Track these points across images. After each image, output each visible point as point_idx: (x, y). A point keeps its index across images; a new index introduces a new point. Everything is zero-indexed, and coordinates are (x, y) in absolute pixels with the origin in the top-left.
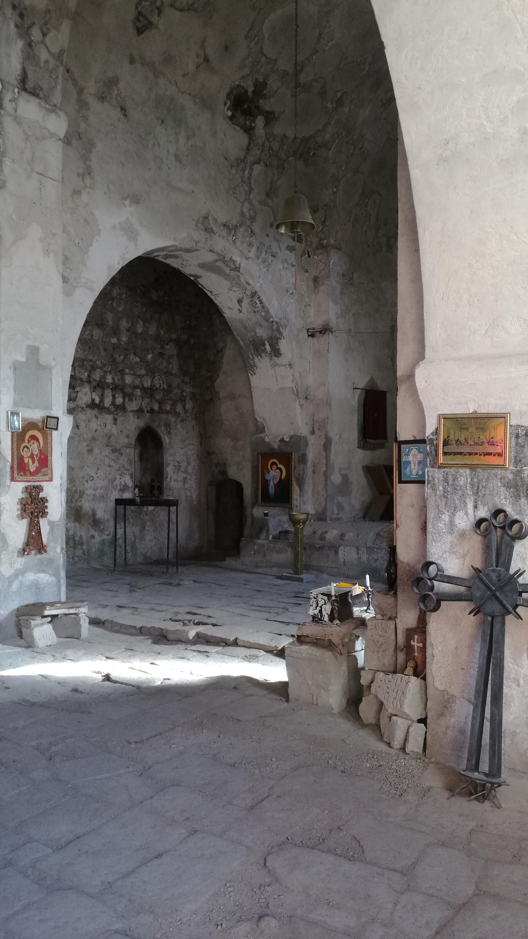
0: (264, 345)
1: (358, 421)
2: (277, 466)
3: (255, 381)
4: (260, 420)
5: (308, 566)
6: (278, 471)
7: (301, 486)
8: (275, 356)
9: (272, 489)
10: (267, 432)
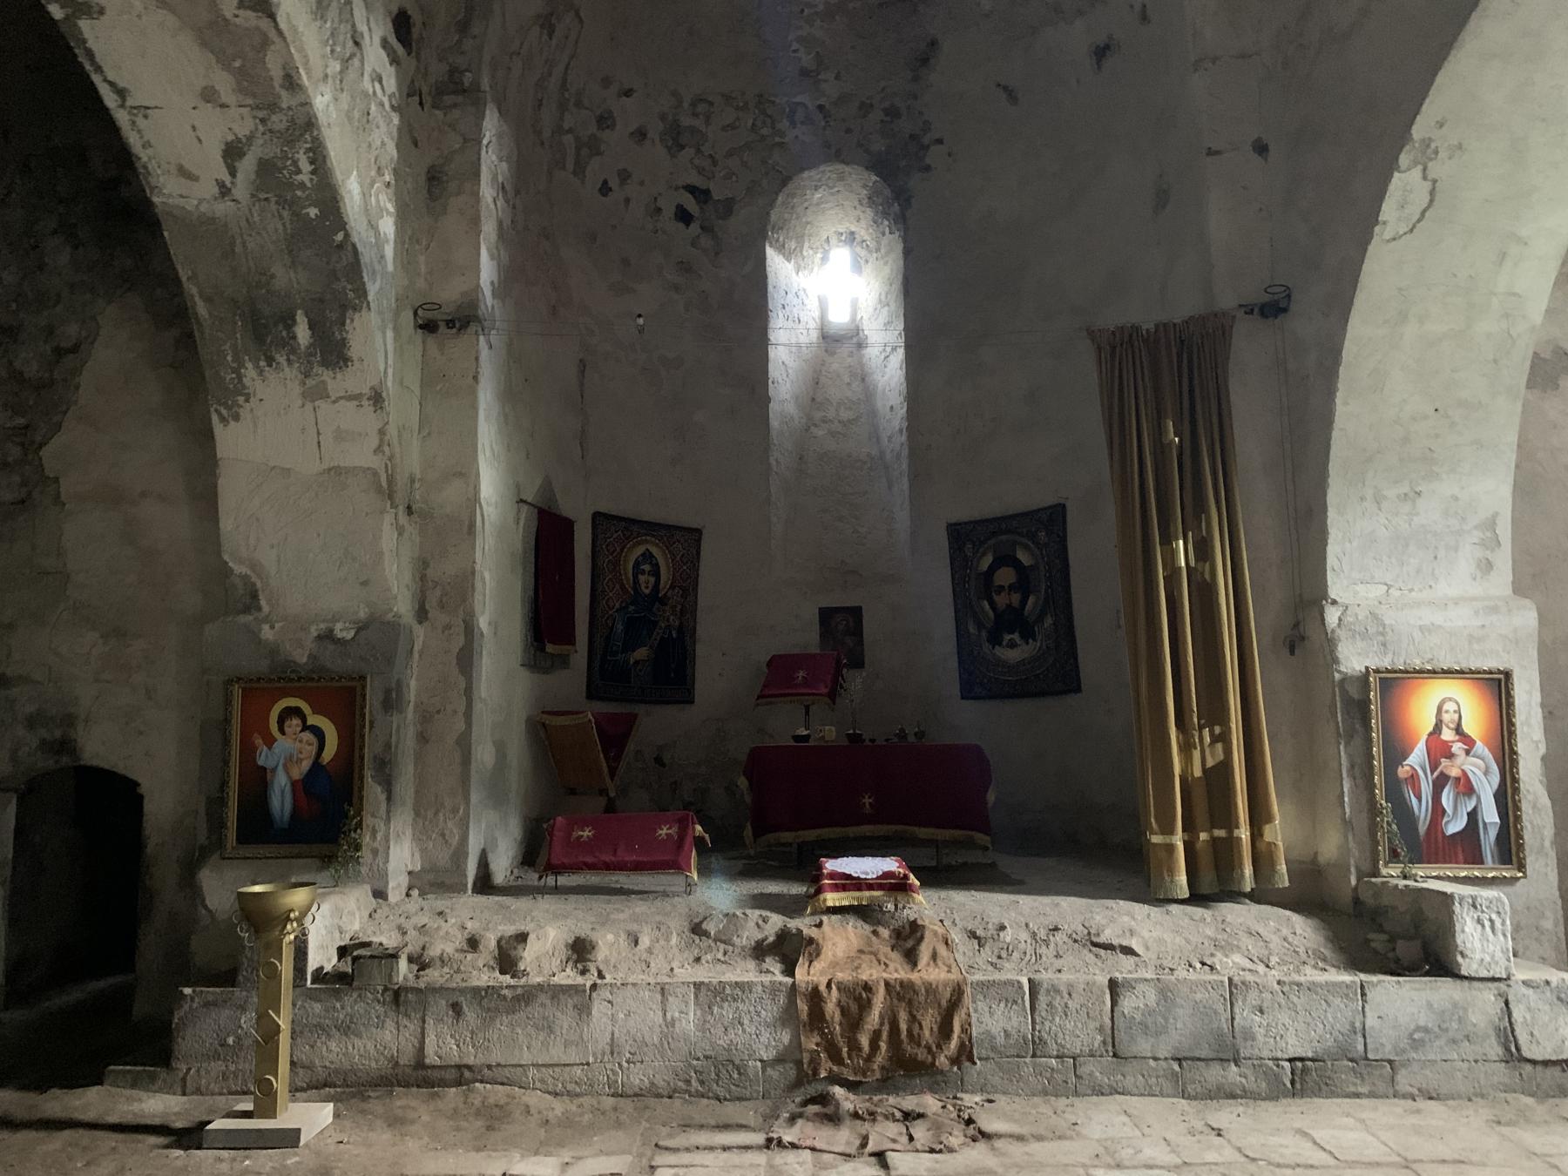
0: (289, 321)
1: (524, 590)
2: (304, 718)
3: (231, 440)
4: (239, 569)
5: (469, 1067)
6: (307, 736)
7: (388, 784)
8: (325, 363)
9: (281, 801)
10: (266, 609)
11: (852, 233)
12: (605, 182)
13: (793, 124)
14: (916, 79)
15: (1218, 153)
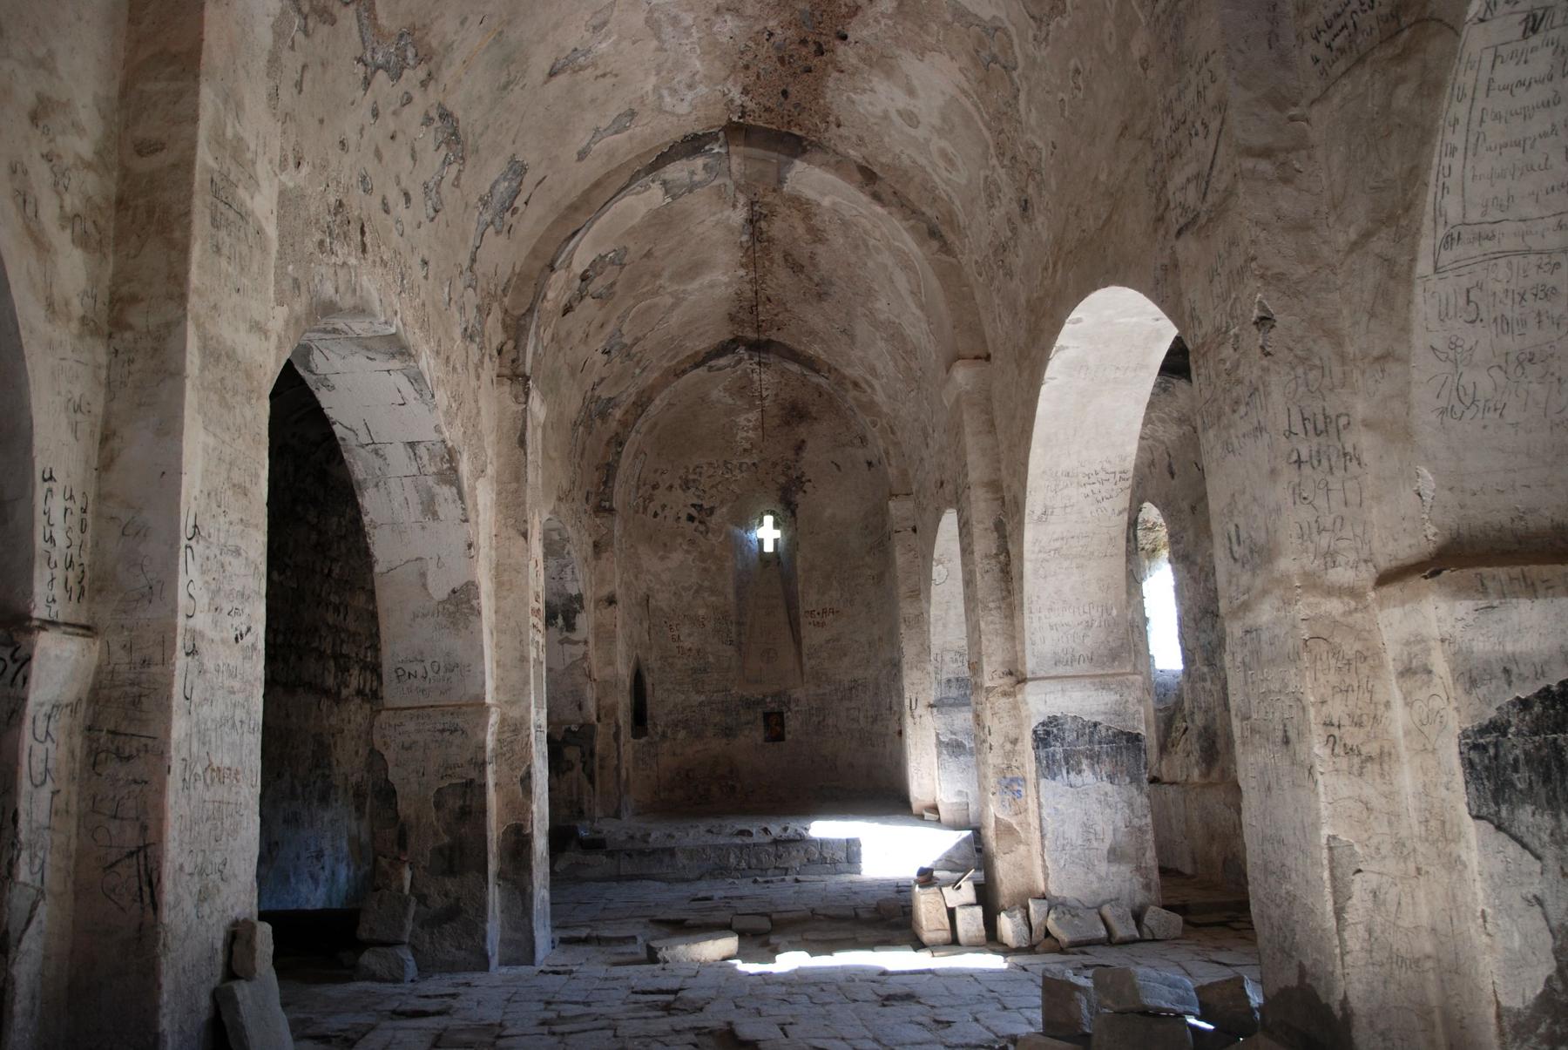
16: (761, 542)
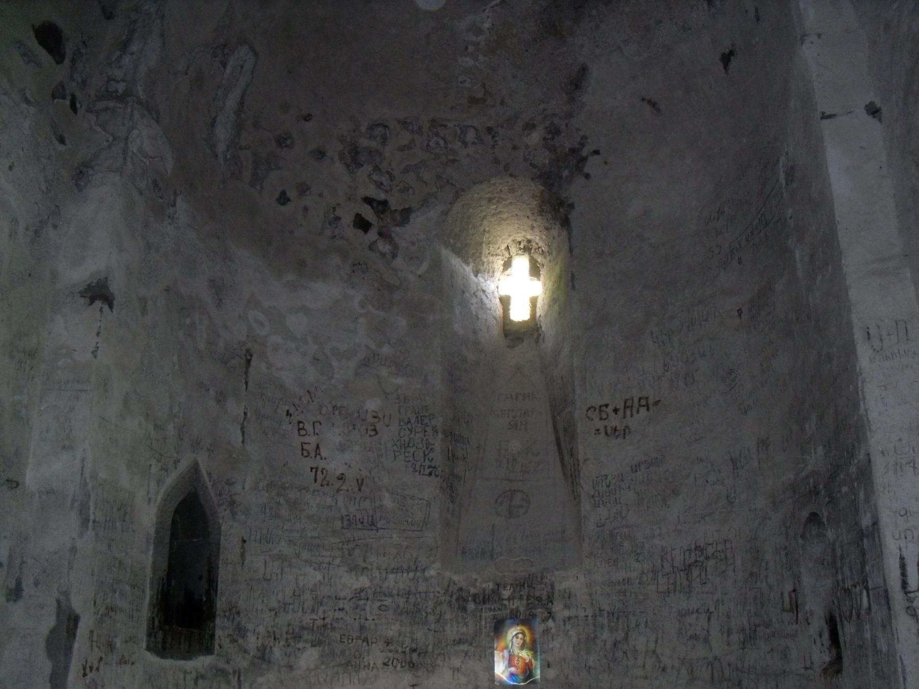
11: (529, 241)
12: (283, 193)
13: (465, 144)
14: (571, 100)
15: (830, 117)
16: (505, 302)
